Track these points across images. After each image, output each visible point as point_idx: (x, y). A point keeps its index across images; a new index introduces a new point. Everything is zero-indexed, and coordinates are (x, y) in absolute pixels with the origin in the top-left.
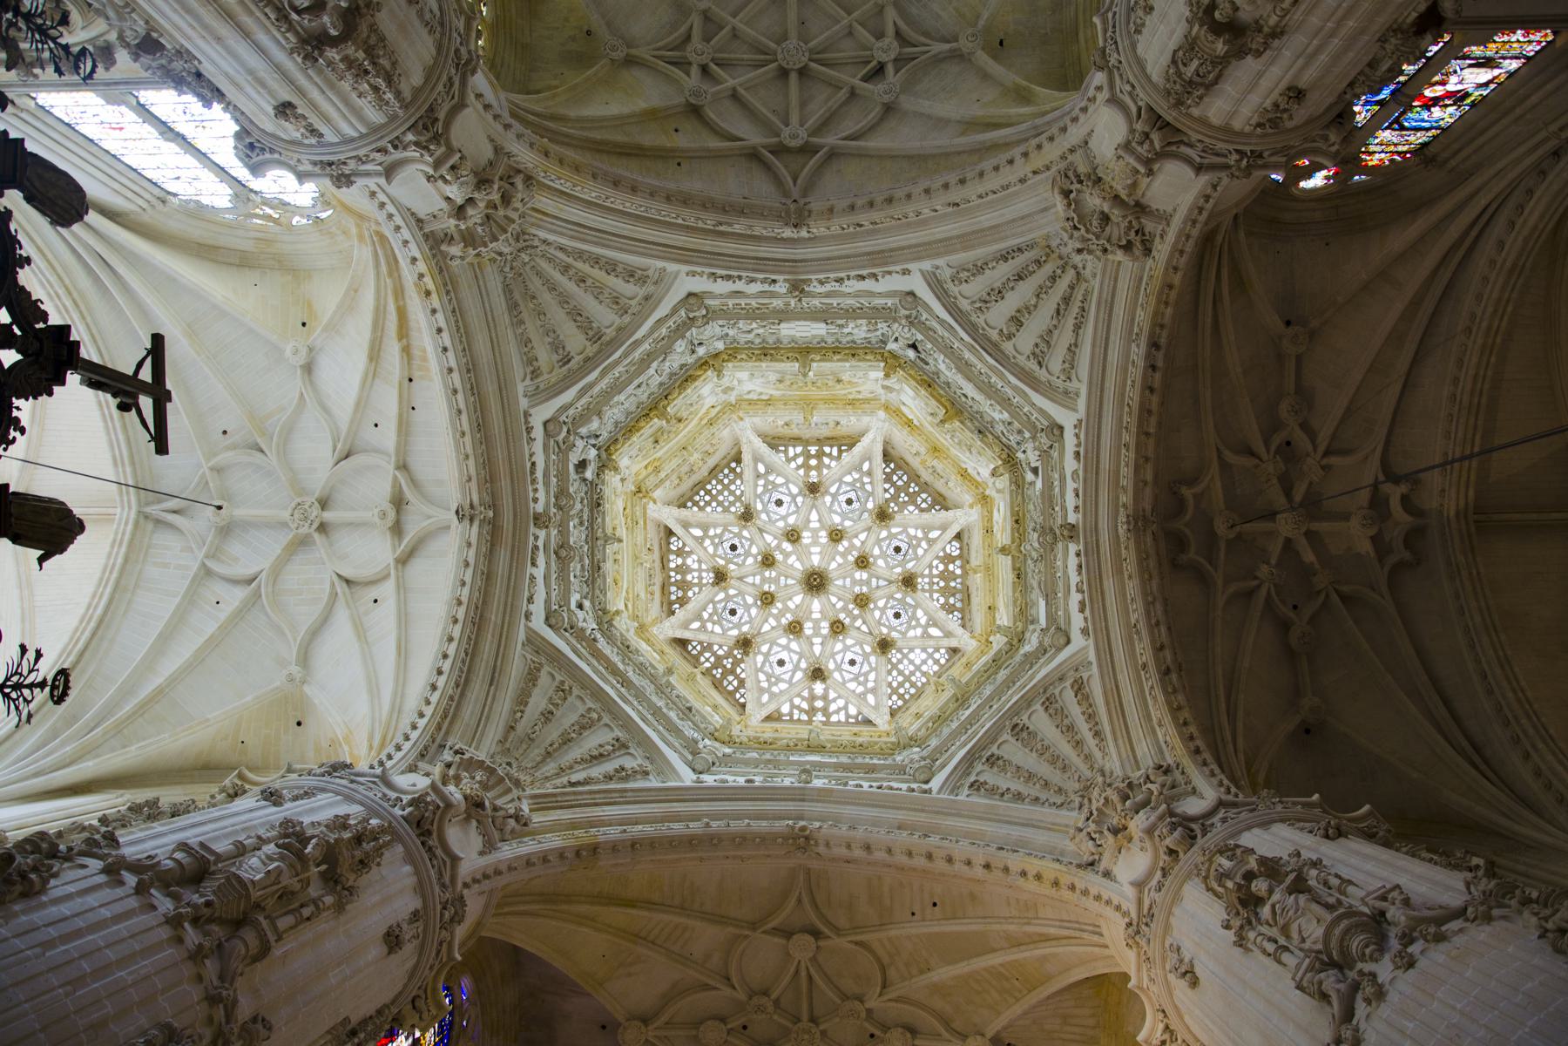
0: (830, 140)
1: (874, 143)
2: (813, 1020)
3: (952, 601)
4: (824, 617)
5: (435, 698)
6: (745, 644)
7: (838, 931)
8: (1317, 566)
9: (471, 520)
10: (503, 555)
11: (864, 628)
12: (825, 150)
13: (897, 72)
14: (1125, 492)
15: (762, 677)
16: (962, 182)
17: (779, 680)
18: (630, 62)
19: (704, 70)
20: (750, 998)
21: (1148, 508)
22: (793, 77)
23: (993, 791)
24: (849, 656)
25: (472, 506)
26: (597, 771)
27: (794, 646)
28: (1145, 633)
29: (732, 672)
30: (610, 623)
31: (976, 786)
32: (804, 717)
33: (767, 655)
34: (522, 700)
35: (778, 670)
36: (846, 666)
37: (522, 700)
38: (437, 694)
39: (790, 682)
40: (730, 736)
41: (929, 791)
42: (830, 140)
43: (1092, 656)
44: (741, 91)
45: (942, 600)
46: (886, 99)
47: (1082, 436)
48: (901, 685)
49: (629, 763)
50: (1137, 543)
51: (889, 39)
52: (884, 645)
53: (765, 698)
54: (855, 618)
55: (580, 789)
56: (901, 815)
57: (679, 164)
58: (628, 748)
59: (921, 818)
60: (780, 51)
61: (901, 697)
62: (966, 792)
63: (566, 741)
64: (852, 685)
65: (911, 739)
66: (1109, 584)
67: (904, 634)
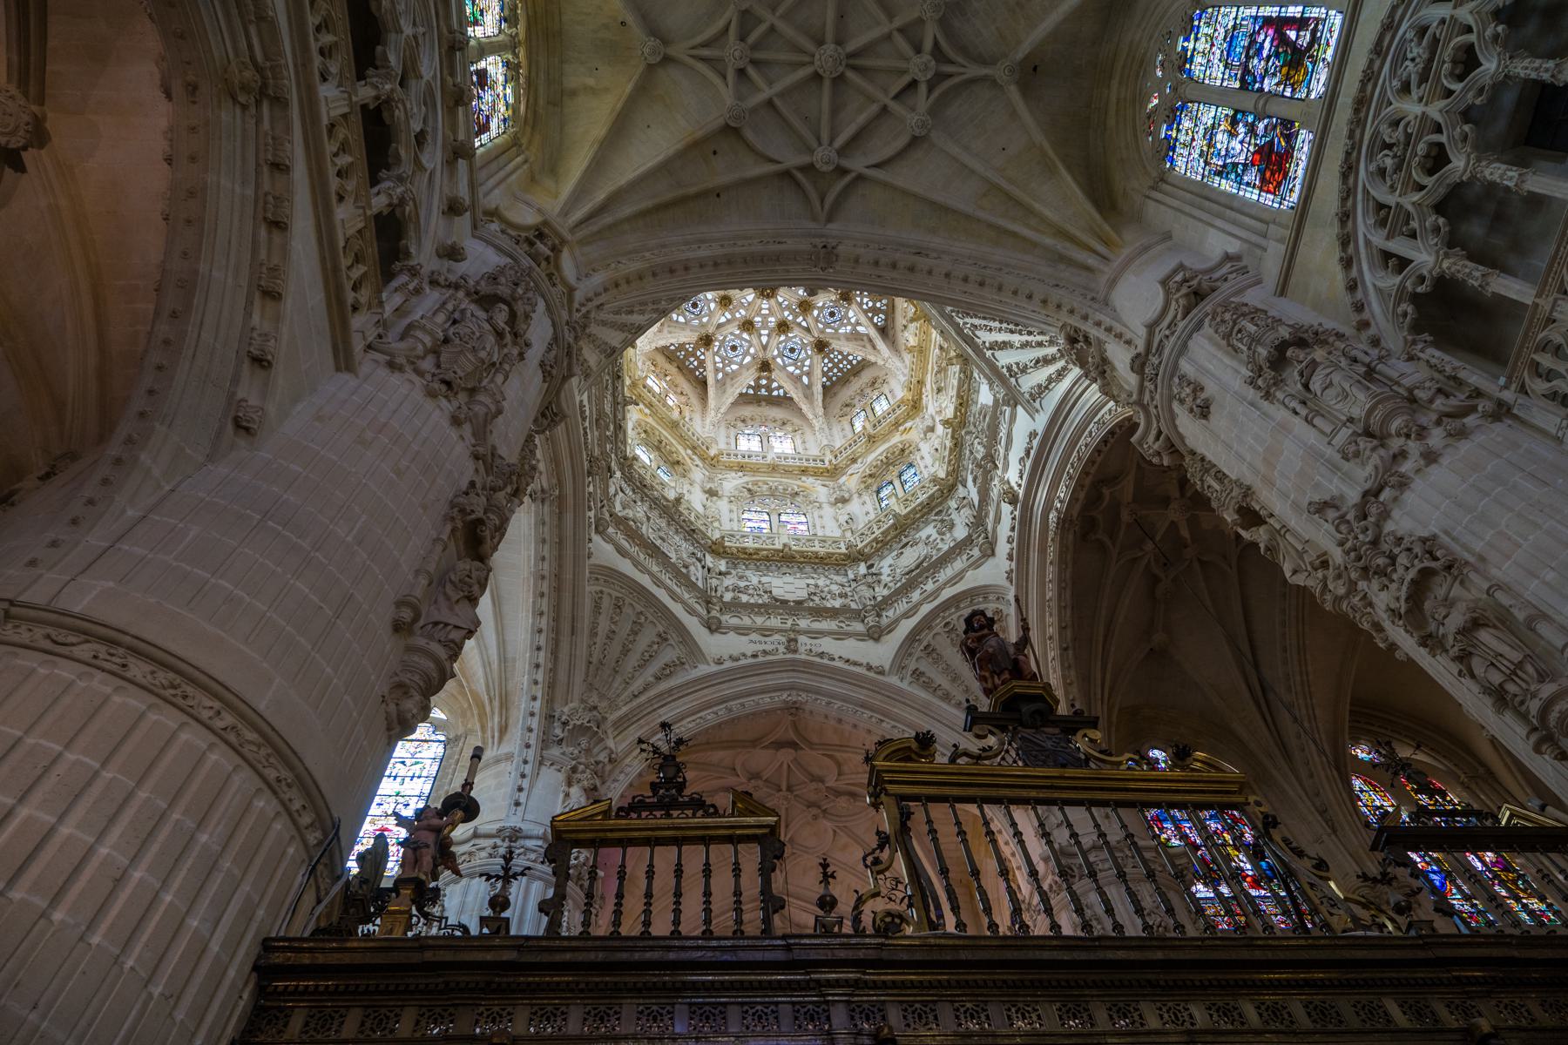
0: (857, 164)
1: (901, 176)
2: (789, 789)
3: (878, 305)
4: (771, 314)
5: (540, 677)
6: (707, 341)
7: (811, 745)
8: (1189, 541)
9: (543, 501)
10: (569, 517)
11: (804, 324)
12: (853, 175)
13: (930, 91)
14: (1061, 502)
15: (717, 359)
16: (982, 284)
17: (731, 363)
18: (667, 60)
19: (741, 72)
20: (750, 779)
21: (1075, 515)
22: (827, 84)
23: (928, 685)
24: (790, 345)
25: (543, 491)
26: (648, 674)
27: (745, 336)
28: (1055, 611)
29: (694, 355)
30: (631, 466)
31: (917, 674)
32: (751, 392)
33: (722, 342)
34: (593, 634)
35: (731, 354)
36: (787, 353)
37: (593, 634)
38: (541, 670)
39: (741, 365)
40: (724, 547)
41: (882, 673)
42: (857, 164)
43: (1011, 597)
44: (778, 102)
45: (870, 304)
46: (917, 132)
47: (1035, 443)
48: (830, 369)
49: (669, 655)
50: (1062, 539)
51: (926, 57)
52: (821, 346)
53: (720, 375)
54: (796, 317)
55: (643, 698)
56: (861, 695)
57: (718, 195)
58: (666, 640)
59: (877, 701)
60: (817, 56)
61: (829, 379)
62: (909, 679)
63: (626, 651)
64: (791, 369)
65: (859, 552)
66: (1034, 556)
67: (836, 330)
